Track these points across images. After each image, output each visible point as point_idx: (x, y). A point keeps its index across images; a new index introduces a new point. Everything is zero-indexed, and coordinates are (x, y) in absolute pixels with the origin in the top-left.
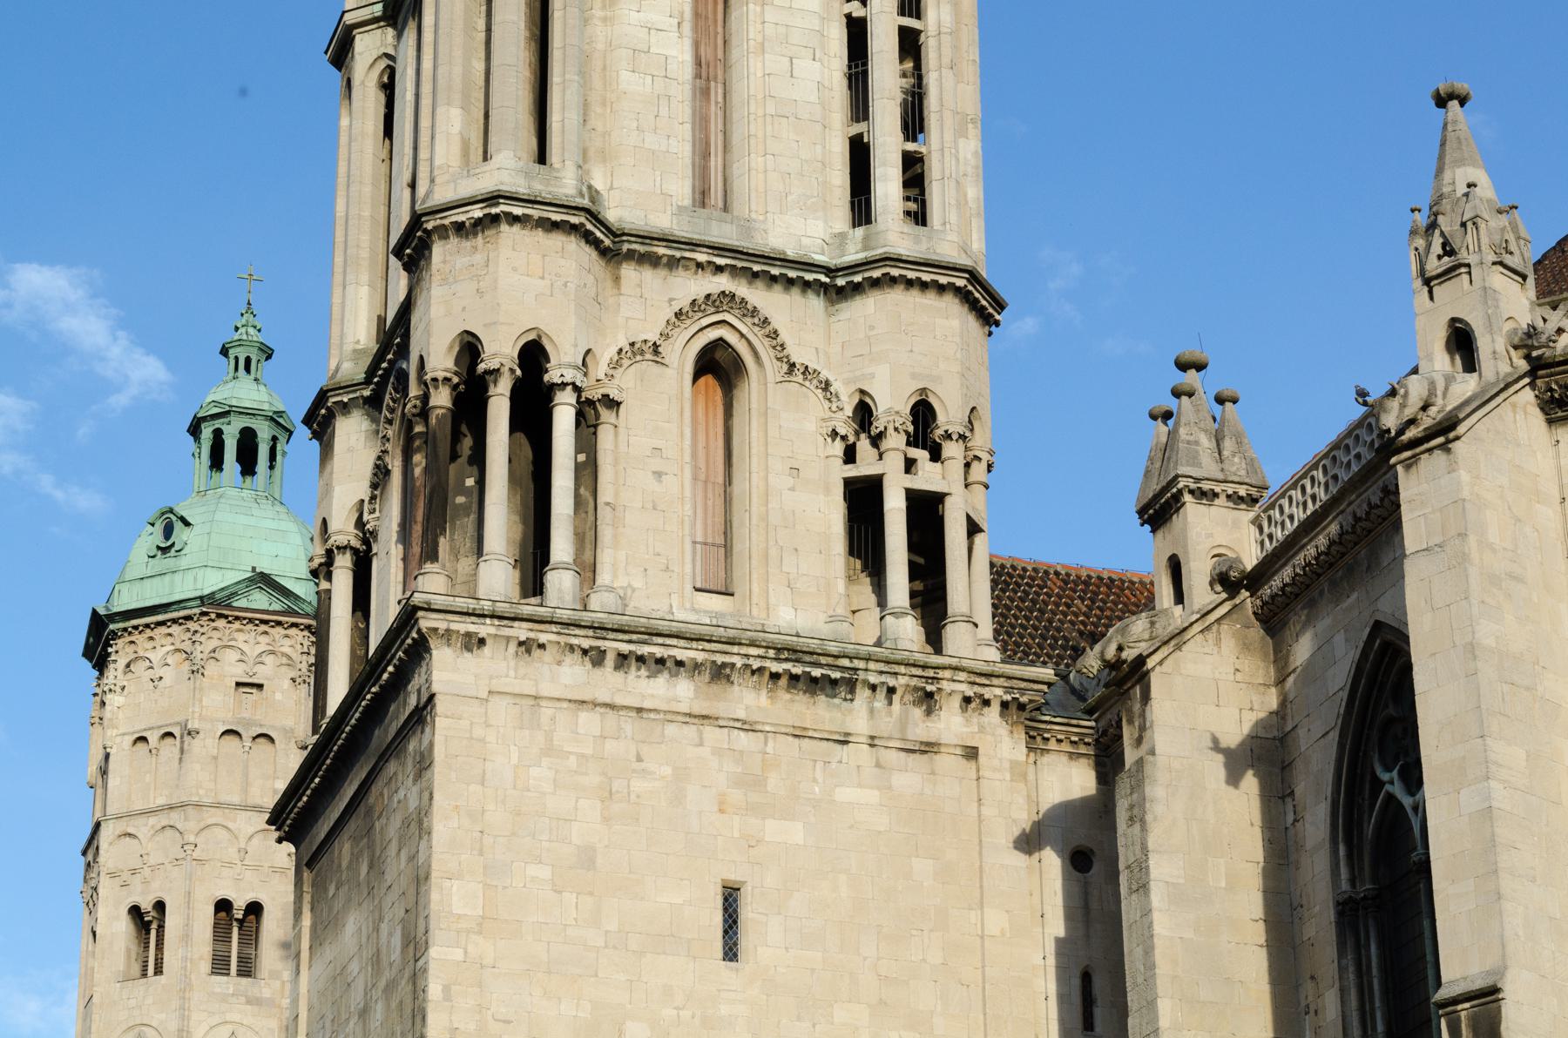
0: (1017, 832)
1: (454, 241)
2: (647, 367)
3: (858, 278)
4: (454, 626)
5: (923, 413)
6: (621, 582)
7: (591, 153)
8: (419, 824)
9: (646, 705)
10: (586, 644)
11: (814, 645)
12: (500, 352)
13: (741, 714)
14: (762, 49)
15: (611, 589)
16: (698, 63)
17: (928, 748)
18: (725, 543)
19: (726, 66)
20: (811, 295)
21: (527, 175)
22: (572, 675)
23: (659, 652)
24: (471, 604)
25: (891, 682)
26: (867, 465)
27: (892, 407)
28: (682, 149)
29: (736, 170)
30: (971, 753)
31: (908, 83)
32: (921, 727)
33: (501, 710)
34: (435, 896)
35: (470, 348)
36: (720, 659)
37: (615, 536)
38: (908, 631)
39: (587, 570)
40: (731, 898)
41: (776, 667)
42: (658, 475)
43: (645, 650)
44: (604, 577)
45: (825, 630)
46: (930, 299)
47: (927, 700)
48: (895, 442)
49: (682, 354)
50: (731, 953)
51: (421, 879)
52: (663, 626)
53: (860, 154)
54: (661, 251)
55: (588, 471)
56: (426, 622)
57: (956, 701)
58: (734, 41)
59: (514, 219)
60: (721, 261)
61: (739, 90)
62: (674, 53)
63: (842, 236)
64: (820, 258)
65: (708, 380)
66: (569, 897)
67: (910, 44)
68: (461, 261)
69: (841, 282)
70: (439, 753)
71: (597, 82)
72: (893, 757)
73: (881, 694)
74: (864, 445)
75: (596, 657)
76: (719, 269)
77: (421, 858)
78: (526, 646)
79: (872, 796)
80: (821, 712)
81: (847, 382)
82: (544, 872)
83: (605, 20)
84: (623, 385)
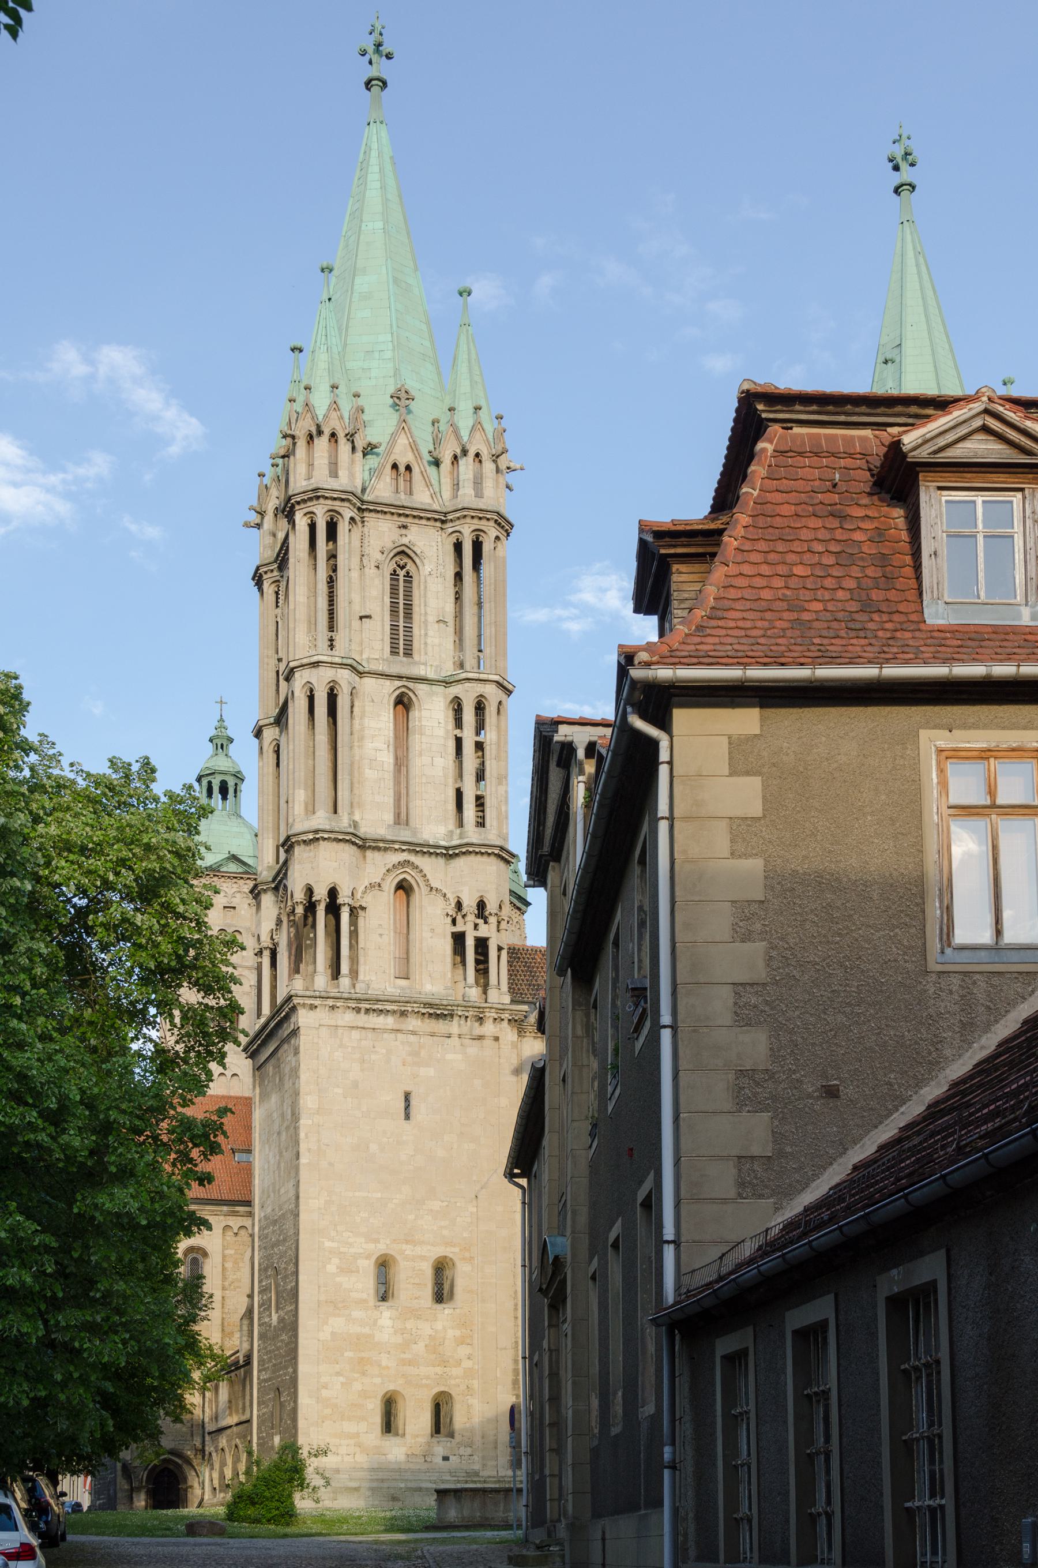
0: (512, 1068)
1: (302, 846)
3: (457, 851)
5: (481, 905)
6: (367, 978)
7: (355, 804)
8: (295, 1071)
10: (354, 1006)
11: (437, 1002)
12: (321, 894)
13: (411, 1028)
14: (421, 755)
15: (363, 982)
16: (396, 758)
17: (481, 1038)
18: (406, 958)
19: (407, 760)
20: (439, 857)
21: (329, 819)
22: (348, 1017)
23: (381, 1007)
24: (312, 994)
25: (467, 1014)
26: (458, 929)
27: (470, 904)
28: (389, 800)
29: (411, 805)
30: (497, 1039)
31: (479, 761)
32: (478, 1030)
33: (324, 1031)
34: (301, 1101)
35: (310, 891)
36: (403, 1009)
38: (474, 994)
39: (354, 973)
40: (407, 1097)
41: (424, 1011)
43: (375, 1007)
44: (361, 977)
45: (444, 992)
46: (485, 858)
47: (480, 1020)
48: (471, 918)
49: (390, 884)
50: (407, 1117)
51: (297, 1094)
52: (382, 998)
53: (459, 794)
54: (381, 845)
55: (354, 934)
56: (296, 1001)
57: (491, 1020)
58: (410, 750)
59: (325, 839)
60: (404, 848)
61: (412, 770)
63: (451, 832)
64: (443, 843)
65: (401, 892)
66: (349, 1100)
67: (479, 746)
68: (306, 855)
69: (451, 852)
70: (302, 1049)
71: (356, 774)
72: (467, 1042)
73: (463, 1019)
74: (459, 918)
75: (358, 1010)
76: (404, 850)
77: (297, 1085)
78: (333, 1007)
79: (459, 1057)
80: (441, 1026)
81: (453, 893)
82: (339, 1091)
83: (359, 747)
84: (367, 901)
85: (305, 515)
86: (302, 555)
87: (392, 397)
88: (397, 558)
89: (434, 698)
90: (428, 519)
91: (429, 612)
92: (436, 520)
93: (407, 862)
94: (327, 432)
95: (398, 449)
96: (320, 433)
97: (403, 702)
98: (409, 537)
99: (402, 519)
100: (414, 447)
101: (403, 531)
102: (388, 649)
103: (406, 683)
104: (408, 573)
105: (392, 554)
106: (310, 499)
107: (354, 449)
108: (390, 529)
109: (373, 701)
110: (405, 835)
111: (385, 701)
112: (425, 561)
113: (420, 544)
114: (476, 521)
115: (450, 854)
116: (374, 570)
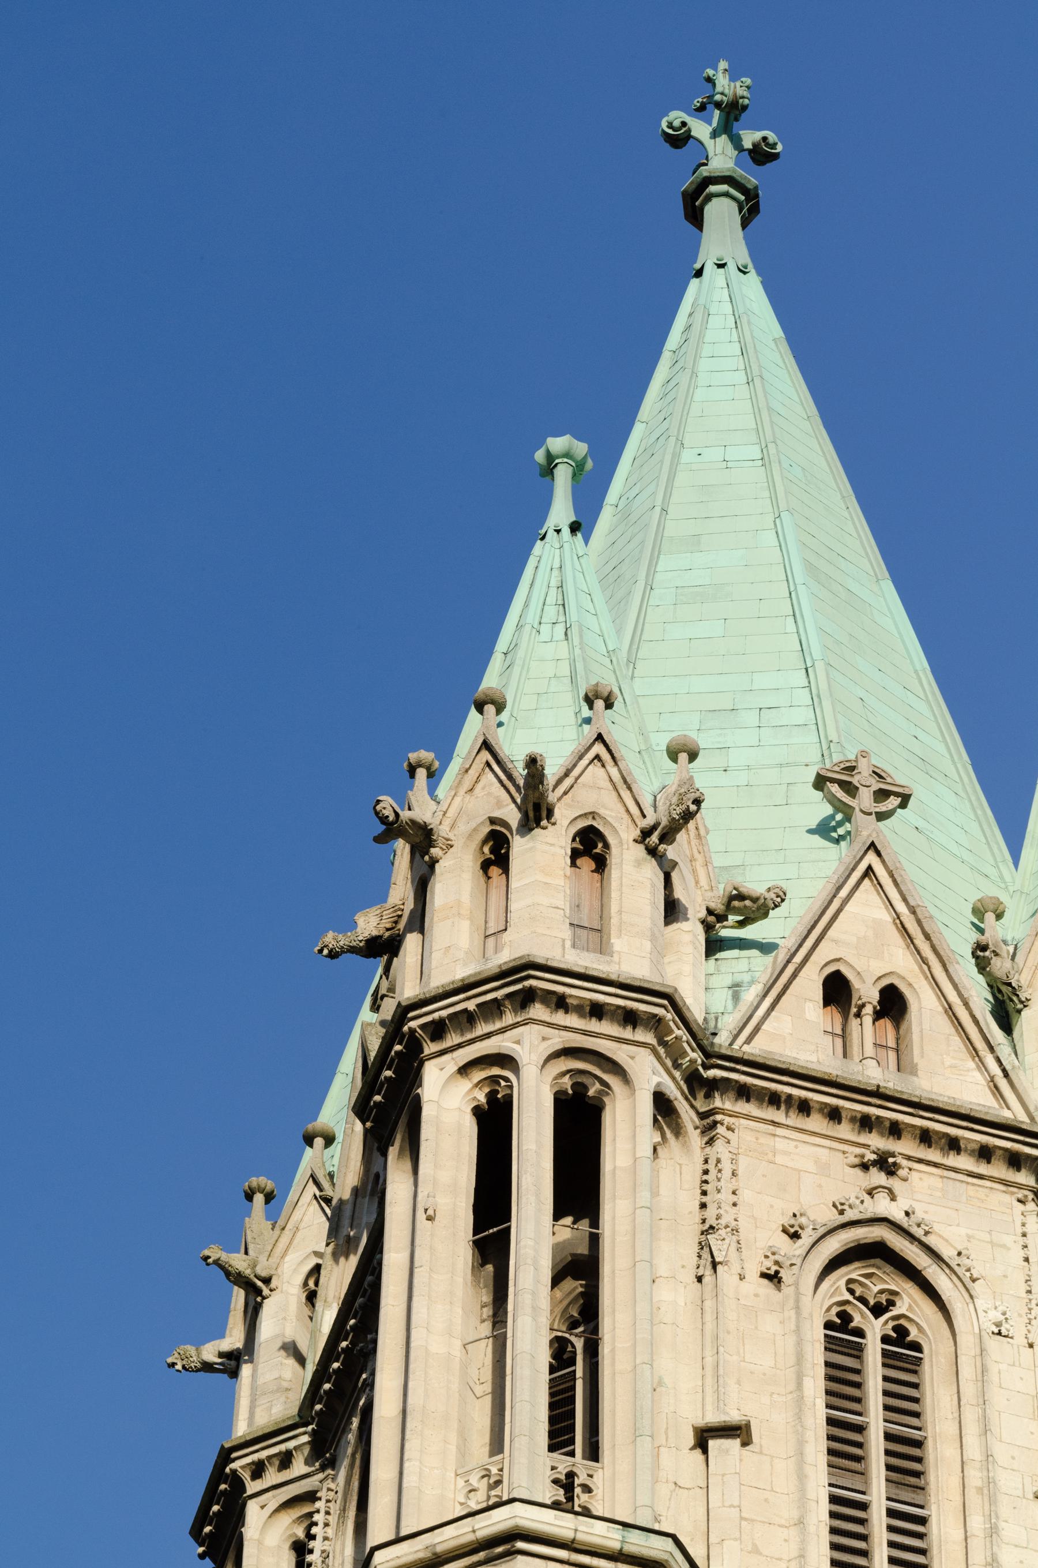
85: (464, 1070)
86: (445, 1176)
87: (820, 782)
90: (985, 1153)
91: (1000, 1452)
99: (877, 1141)
104: (901, 1332)
105: (834, 1245)
106: (492, 1009)
107: (672, 910)
112: (977, 1288)
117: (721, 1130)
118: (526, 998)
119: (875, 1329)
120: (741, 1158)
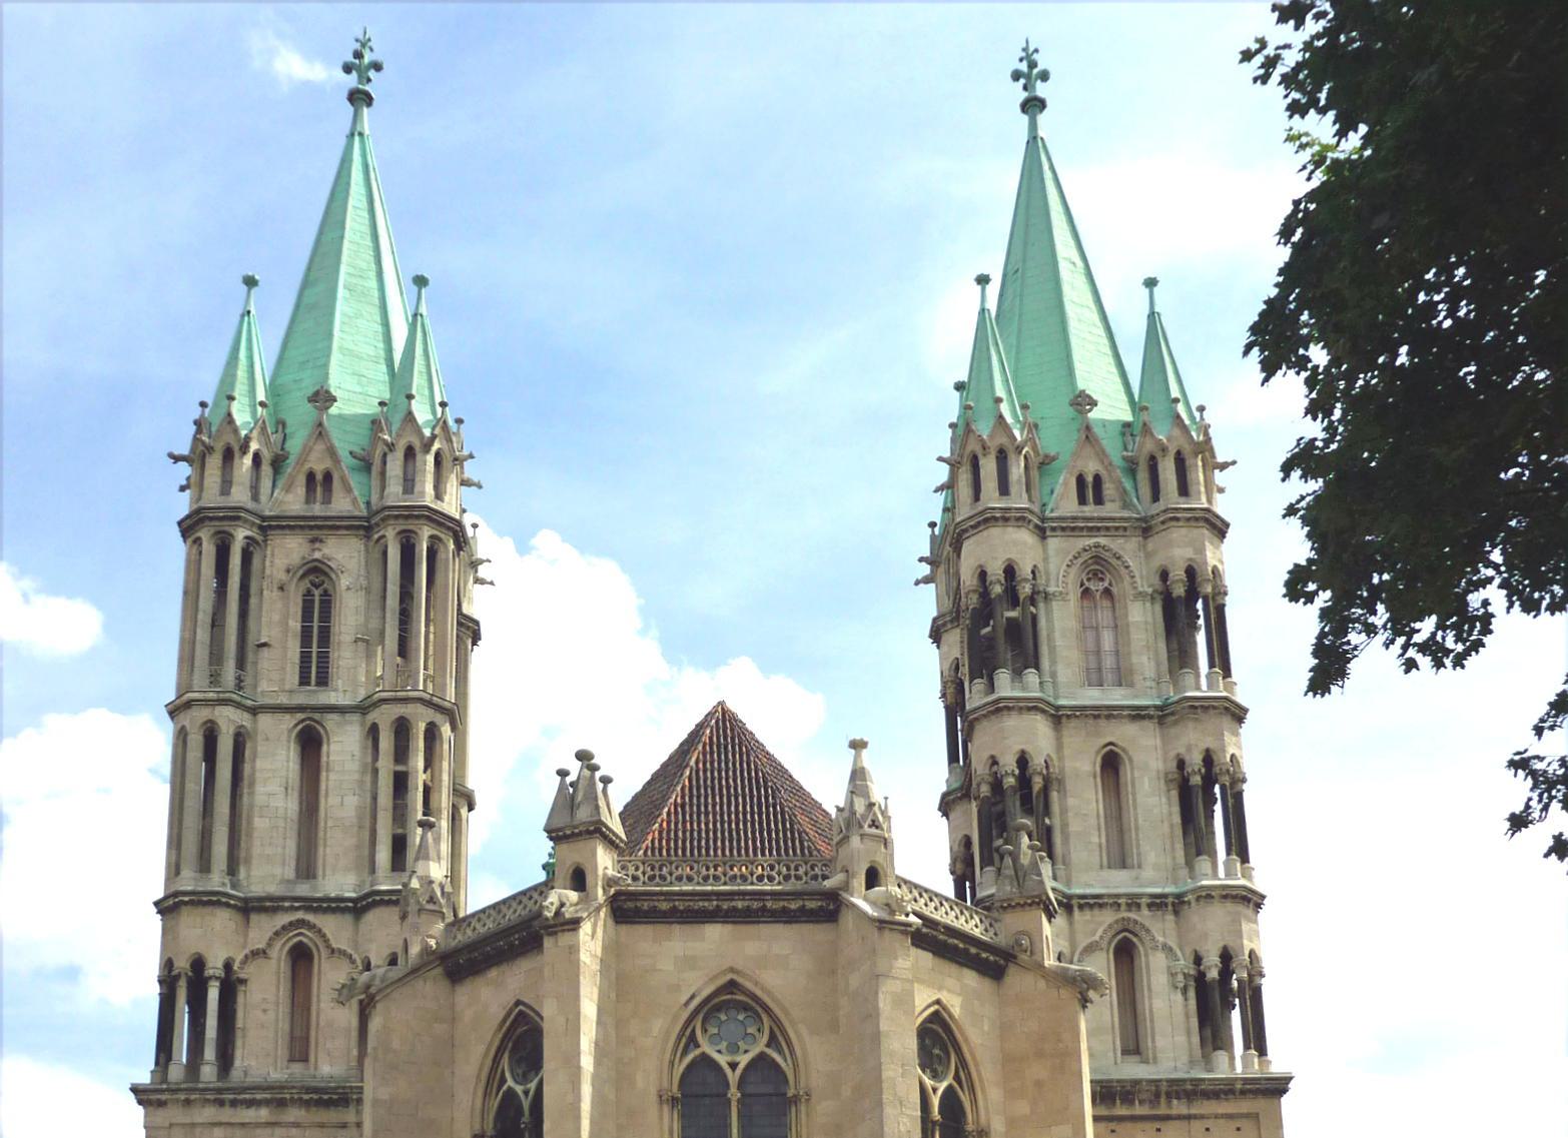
2: (260, 961)
4: (151, 1097)
9: (247, 1121)
13: (292, 1120)
22: (208, 1113)
37: (244, 1043)
41: (306, 1097)
42: (265, 1011)
49: (279, 953)
59: (186, 903)
60: (296, 904)
62: (279, 805)
75: (221, 1103)
88: (311, 577)
89: (348, 728)
92: (358, 528)
93: (301, 923)
94: (219, 447)
95: (313, 456)
96: (210, 449)
97: (310, 743)
98: (326, 551)
100: (332, 452)
101: (317, 545)
102: (296, 679)
103: (310, 715)
104: (326, 591)
105: (301, 572)
108: (300, 544)
109: (267, 739)
110: (303, 890)
111: (284, 737)
113: (339, 557)
114: (401, 521)
115: (359, 907)
116: (276, 593)
117: (269, 542)
118: (202, 520)
119: (317, 593)
120: (276, 550)
